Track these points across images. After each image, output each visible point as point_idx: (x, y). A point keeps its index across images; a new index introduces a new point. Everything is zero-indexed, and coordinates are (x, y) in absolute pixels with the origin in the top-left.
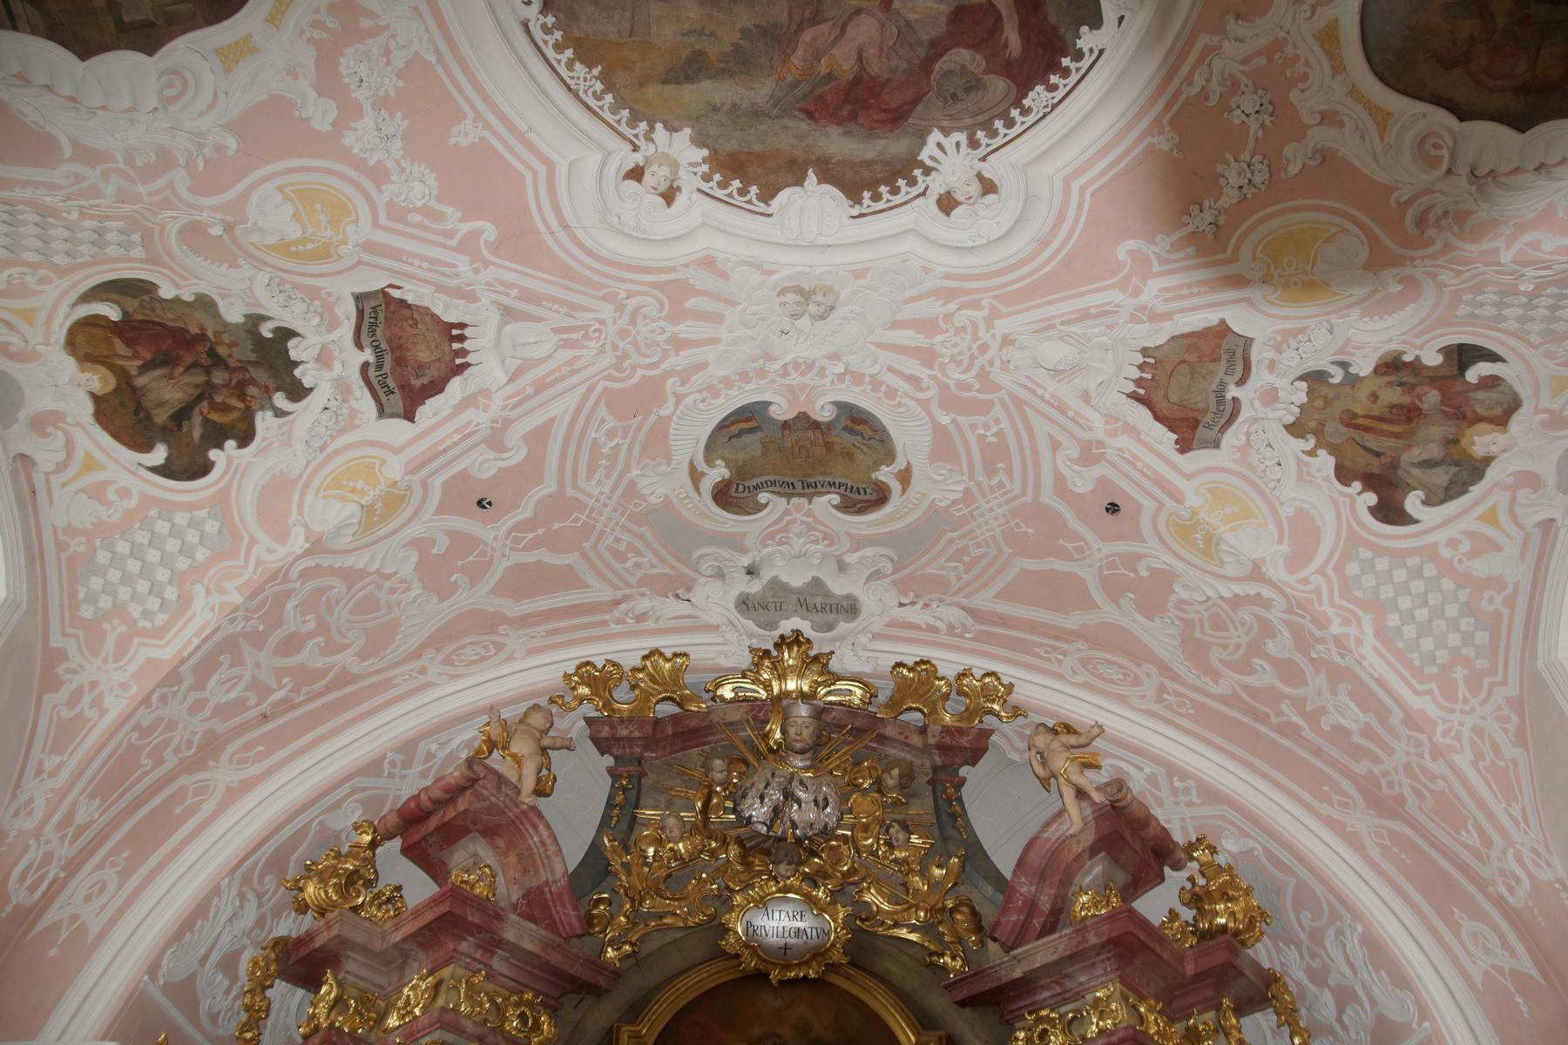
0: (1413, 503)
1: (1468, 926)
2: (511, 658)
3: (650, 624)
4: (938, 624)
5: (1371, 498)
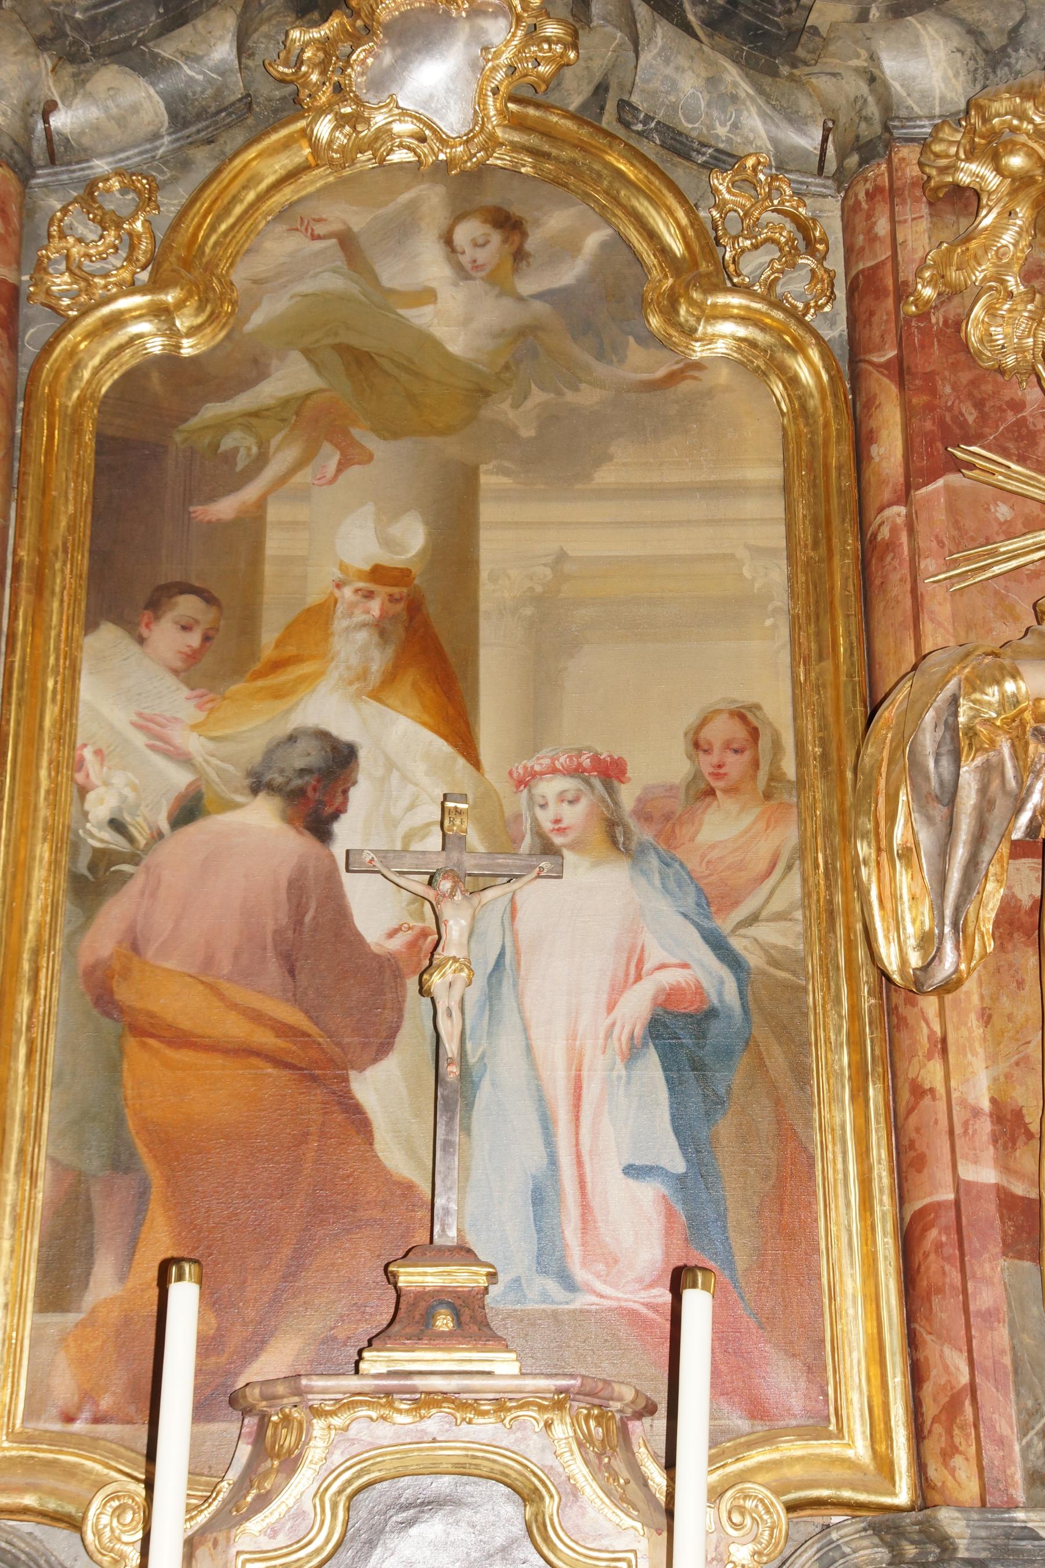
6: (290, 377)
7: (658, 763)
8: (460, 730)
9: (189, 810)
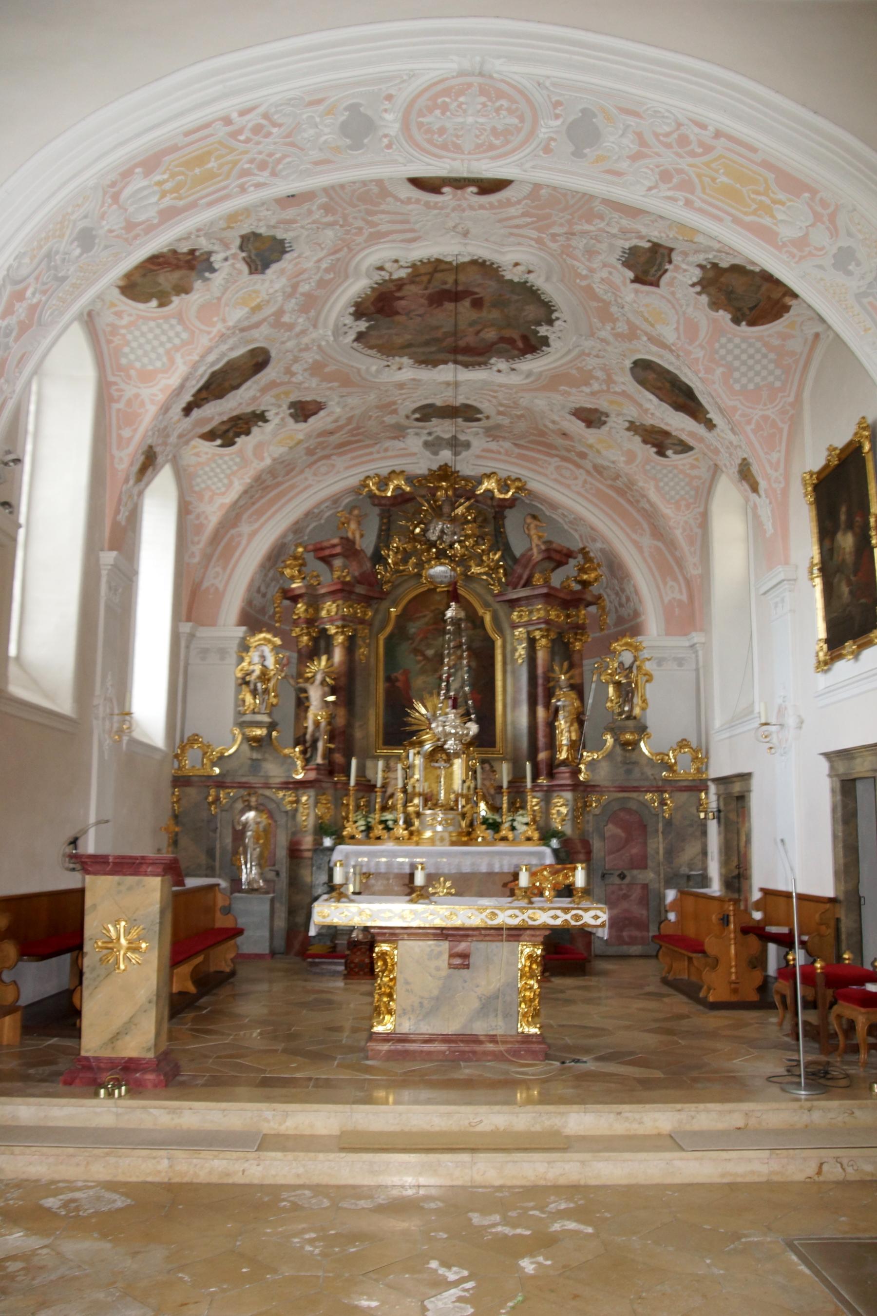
0: (669, 453)
1: (671, 583)
2: (338, 472)
3: (389, 454)
4: (502, 450)
5: (654, 450)
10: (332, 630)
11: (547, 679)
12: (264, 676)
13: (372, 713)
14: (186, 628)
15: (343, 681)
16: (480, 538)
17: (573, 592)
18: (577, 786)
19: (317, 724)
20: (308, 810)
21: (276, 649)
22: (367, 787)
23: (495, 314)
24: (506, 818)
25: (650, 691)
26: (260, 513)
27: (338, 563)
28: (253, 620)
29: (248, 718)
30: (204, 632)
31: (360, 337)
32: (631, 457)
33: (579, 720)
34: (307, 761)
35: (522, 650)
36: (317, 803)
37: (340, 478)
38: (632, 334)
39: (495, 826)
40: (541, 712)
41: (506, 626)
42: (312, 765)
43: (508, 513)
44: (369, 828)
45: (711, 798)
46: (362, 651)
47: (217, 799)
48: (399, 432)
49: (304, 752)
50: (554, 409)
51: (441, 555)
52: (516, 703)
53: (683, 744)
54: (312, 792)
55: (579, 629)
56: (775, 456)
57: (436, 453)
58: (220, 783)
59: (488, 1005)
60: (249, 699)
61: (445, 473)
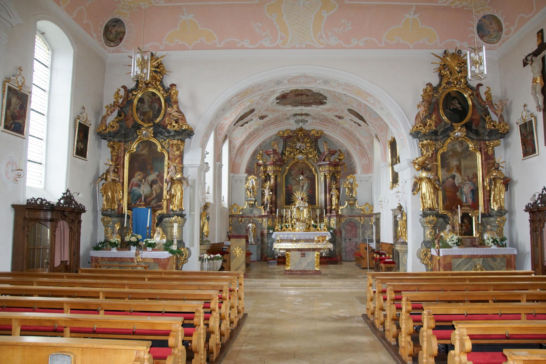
1: (364, 159)
6: (450, 153)
7: (471, 176)
8: (461, 174)
9: (447, 179)
10: (271, 174)
11: (330, 187)
12: (253, 188)
13: (282, 196)
14: (232, 174)
15: (274, 188)
16: (311, 147)
17: (336, 162)
18: (338, 215)
19: (267, 200)
20: (265, 223)
21: (256, 180)
22: (281, 217)
23: (312, 98)
24: (319, 224)
25: (357, 189)
26: (250, 142)
27: (272, 156)
28: (249, 172)
29: (249, 199)
30: (236, 175)
31: (277, 103)
32: (351, 126)
33: (338, 198)
34: (265, 210)
35: (322, 178)
36: (268, 221)
37: (272, 131)
38: (346, 104)
39: (315, 227)
40: (328, 195)
41: (318, 171)
42: (266, 211)
43: (319, 140)
44: (282, 228)
45: (373, 219)
46: (279, 179)
47: (241, 221)
48: (288, 119)
49: (264, 208)
50: (331, 115)
51: (301, 152)
52: (321, 193)
53: (367, 204)
54: (266, 218)
55: (338, 172)
56: (383, 134)
57: (298, 124)
58: (242, 216)
59: (308, 264)
60: (249, 193)
61: (301, 129)
